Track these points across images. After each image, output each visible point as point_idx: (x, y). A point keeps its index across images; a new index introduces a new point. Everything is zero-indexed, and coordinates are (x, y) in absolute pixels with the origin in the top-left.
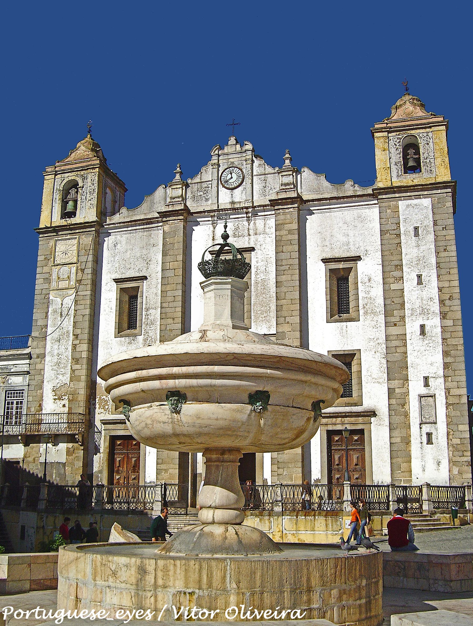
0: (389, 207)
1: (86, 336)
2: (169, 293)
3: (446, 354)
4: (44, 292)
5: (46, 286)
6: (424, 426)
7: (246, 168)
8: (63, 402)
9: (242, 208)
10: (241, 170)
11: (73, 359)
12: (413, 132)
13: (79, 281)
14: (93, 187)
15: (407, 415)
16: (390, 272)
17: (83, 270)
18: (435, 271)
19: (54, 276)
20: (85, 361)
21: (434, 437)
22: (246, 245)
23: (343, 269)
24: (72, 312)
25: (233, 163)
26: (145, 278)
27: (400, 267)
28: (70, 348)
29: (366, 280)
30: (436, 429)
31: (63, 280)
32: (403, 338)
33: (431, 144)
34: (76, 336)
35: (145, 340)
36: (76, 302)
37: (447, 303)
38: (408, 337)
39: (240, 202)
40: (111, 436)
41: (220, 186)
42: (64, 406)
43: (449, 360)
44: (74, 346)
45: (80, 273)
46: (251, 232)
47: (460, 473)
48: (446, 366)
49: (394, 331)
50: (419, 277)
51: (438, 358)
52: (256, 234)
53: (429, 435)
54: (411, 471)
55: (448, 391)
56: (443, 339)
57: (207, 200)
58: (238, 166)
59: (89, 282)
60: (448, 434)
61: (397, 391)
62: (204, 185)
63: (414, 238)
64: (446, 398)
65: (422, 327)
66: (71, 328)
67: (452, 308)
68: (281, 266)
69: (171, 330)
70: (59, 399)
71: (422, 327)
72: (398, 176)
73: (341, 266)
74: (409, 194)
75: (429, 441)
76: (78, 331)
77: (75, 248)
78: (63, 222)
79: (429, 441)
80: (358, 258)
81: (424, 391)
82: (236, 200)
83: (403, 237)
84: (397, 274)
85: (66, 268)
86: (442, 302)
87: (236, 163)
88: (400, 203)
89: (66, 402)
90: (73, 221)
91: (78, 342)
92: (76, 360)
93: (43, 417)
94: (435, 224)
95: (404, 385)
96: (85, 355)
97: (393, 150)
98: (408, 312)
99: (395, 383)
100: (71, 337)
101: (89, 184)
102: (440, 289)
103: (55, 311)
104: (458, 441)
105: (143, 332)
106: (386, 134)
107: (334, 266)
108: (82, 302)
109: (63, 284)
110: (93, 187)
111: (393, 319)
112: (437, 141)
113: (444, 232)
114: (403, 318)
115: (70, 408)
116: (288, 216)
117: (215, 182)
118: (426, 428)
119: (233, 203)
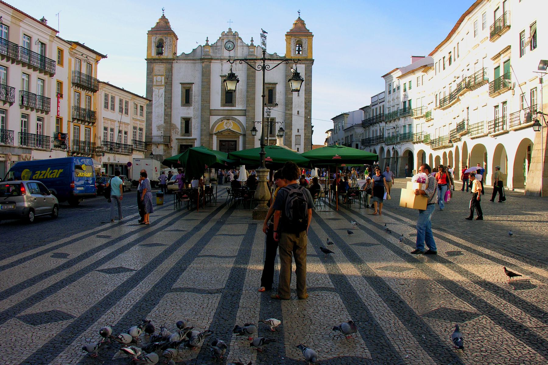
3: (305, 121)
4: (150, 86)
5: (151, 84)
6: (296, 145)
8: (161, 132)
10: (233, 43)
13: (166, 83)
14: (170, 43)
15: (291, 142)
16: (288, 91)
18: (304, 92)
19: (155, 80)
21: (299, 149)
23: (271, 87)
24: (163, 96)
26: (194, 83)
29: (279, 92)
30: (301, 147)
33: (307, 43)
34: (166, 105)
37: (307, 103)
40: (181, 145)
41: (224, 48)
42: (162, 133)
43: (306, 124)
44: (165, 110)
45: (166, 80)
46: (237, 69)
52: (239, 70)
55: (305, 134)
57: (219, 54)
61: (288, 133)
62: (218, 47)
64: (305, 137)
65: (298, 112)
69: (206, 106)
71: (298, 112)
73: (271, 86)
76: (167, 104)
77: (163, 69)
78: (157, 57)
80: (277, 83)
81: (298, 134)
82: (231, 56)
85: (160, 77)
86: (305, 103)
87: (231, 40)
90: (162, 57)
91: (167, 108)
93: (153, 137)
95: (290, 131)
100: (164, 106)
101: (169, 41)
102: (305, 99)
103: (156, 95)
105: (193, 105)
106: (290, 37)
109: (159, 84)
111: (288, 108)
113: (308, 78)
118: (297, 146)
119: (230, 57)
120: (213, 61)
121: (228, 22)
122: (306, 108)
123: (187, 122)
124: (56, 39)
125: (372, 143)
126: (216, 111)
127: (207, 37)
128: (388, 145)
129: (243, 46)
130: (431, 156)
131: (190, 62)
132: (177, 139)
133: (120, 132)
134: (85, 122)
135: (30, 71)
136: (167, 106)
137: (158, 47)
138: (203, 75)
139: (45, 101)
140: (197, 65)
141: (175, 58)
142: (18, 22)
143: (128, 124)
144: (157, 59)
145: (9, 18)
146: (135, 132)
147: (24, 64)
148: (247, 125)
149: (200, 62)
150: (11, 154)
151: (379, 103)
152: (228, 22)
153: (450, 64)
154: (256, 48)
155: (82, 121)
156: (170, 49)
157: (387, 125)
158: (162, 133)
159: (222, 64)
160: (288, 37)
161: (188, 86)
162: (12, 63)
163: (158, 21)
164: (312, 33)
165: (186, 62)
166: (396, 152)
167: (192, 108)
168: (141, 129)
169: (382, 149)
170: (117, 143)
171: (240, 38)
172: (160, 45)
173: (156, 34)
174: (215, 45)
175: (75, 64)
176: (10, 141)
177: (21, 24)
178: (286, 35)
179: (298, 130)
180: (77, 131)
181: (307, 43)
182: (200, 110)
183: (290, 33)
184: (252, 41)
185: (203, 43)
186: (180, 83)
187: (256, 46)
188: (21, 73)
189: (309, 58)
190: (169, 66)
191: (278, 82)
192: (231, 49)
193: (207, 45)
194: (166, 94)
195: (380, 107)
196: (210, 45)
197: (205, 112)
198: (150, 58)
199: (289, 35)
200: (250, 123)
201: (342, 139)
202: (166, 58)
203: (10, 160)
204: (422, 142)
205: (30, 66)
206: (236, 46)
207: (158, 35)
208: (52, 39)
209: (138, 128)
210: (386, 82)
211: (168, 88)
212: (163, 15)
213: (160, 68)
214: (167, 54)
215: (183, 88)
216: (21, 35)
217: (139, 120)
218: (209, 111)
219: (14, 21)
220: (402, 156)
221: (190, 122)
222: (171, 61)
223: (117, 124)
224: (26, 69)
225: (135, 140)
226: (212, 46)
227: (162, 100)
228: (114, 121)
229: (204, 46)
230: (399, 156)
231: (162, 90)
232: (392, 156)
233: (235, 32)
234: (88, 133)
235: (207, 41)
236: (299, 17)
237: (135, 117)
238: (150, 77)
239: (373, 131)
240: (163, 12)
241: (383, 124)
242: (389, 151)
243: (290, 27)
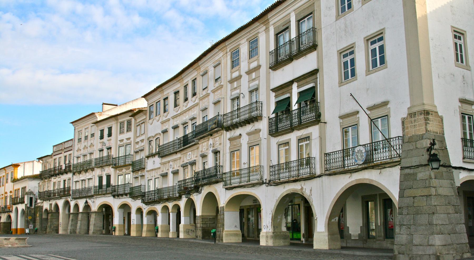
125: (53, 196)
128: (75, 199)
130: (140, 211)
151: (65, 152)
153: (176, 106)
157: (75, 177)
166: (87, 207)
169: (67, 204)
195: (65, 157)
201: (11, 192)
204: (126, 195)
210: (75, 130)
220: (96, 211)
230: (92, 211)
232: (81, 210)
239: (54, 183)
241: (70, 175)
242: (77, 206)
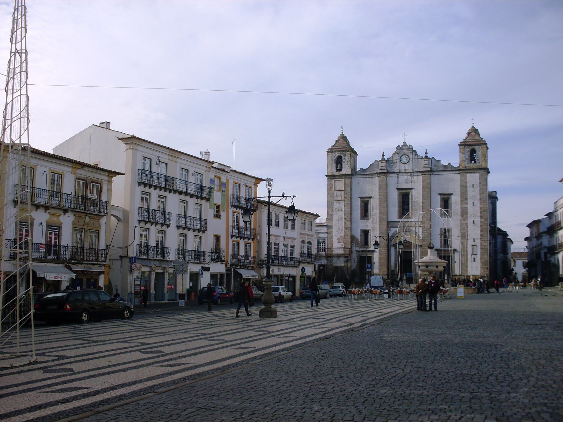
0: (464, 176)
1: (349, 219)
2: (382, 205)
3: (481, 231)
4: (331, 201)
5: (331, 199)
7: (410, 156)
9: (409, 172)
10: (408, 156)
11: (345, 228)
12: (474, 147)
15: (467, 252)
17: (346, 193)
19: (335, 195)
20: (350, 229)
22: (411, 187)
23: (447, 198)
25: (404, 153)
26: (372, 197)
27: (466, 199)
28: (343, 223)
31: (339, 196)
32: (467, 225)
34: (345, 219)
35: (372, 221)
36: (345, 206)
37: (483, 213)
38: (468, 224)
39: (408, 170)
42: (342, 245)
43: (482, 233)
44: (345, 223)
46: (412, 181)
47: (484, 271)
48: (481, 235)
49: (464, 222)
50: (473, 203)
51: (479, 232)
53: (474, 258)
54: (467, 270)
55: (481, 244)
56: (481, 226)
57: (395, 167)
58: (408, 155)
59: (349, 198)
60: (481, 258)
62: (394, 161)
63: (472, 188)
65: (474, 221)
66: (343, 216)
67: (485, 215)
68: (424, 196)
69: (383, 219)
70: (340, 243)
71: (474, 221)
72: (468, 164)
73: (446, 197)
74: (471, 171)
75: (474, 261)
76: (346, 217)
77: (343, 184)
78: (337, 173)
79: (474, 261)
80: (452, 194)
81: (473, 243)
82: (406, 168)
83: (468, 188)
84: (466, 201)
85: (340, 192)
86: (481, 212)
87: (406, 153)
88: (468, 174)
89: (343, 244)
90: (341, 173)
92: (346, 228)
94: (480, 183)
96: (349, 226)
97: (466, 154)
98: (468, 215)
99: (463, 241)
100: (344, 219)
101: (347, 158)
102: (481, 208)
103: (336, 209)
104: (484, 261)
106: (464, 147)
107: (443, 196)
108: (347, 206)
109: (339, 198)
110: (349, 159)
111: (464, 218)
112: (483, 151)
113: (483, 187)
114: (467, 218)
115: (344, 246)
116: (426, 177)
117: (398, 161)
118: (473, 256)
119: (405, 170)
120: (388, 175)
121: (402, 136)
122: (481, 217)
123: (366, 233)
124: (212, 169)
126: (393, 223)
127: (383, 152)
129: (417, 159)
131: (367, 176)
132: (357, 251)
133: (286, 246)
134: (244, 238)
135: (187, 198)
136: (347, 219)
137: (337, 164)
138: (380, 189)
139: (202, 221)
140: (374, 179)
141: (354, 173)
142: (175, 159)
143: (295, 239)
144: (337, 175)
145: (167, 157)
146: (304, 246)
147: (180, 193)
148: (423, 236)
149: (377, 176)
150: (168, 267)
152: (402, 136)
154: (430, 160)
155: (241, 238)
156: (349, 166)
158: (342, 245)
159: (398, 177)
160: (461, 147)
161: (367, 199)
162: (170, 192)
163: (337, 139)
164: (485, 141)
165: (364, 177)
167: (370, 220)
168: (310, 243)
170: (281, 257)
171: (415, 151)
172: (339, 162)
173: (335, 151)
174: (391, 159)
175: (234, 189)
176: (166, 256)
177: (178, 160)
178: (460, 145)
179: (474, 239)
180: (236, 246)
181: (480, 152)
182: (378, 222)
183: (463, 143)
184: (426, 153)
185: (380, 158)
186: (359, 197)
187: (430, 158)
188: (178, 201)
189: (484, 166)
190: (348, 181)
191: (453, 193)
192: (406, 162)
193: (383, 160)
194: (345, 208)
196: (386, 159)
197: (383, 225)
198: (331, 174)
199: (463, 145)
200: (426, 234)
202: (345, 174)
203: (167, 271)
205: (186, 194)
206: (411, 160)
207: (337, 153)
208: (208, 169)
209: (306, 242)
211: (347, 202)
212: (342, 133)
213: (340, 184)
214: (346, 170)
215: (362, 202)
216: (178, 169)
217: (307, 235)
218: (386, 223)
219: (171, 158)
221: (369, 233)
222: (350, 177)
223: (282, 239)
224: (183, 197)
225: (303, 253)
226: (387, 161)
227: (342, 214)
228: (279, 236)
229: (380, 161)
231: (342, 205)
233: (410, 145)
234: (247, 247)
235: (383, 156)
236: (473, 126)
237: (303, 231)
238: (331, 192)
240: (342, 131)
243: (463, 136)
